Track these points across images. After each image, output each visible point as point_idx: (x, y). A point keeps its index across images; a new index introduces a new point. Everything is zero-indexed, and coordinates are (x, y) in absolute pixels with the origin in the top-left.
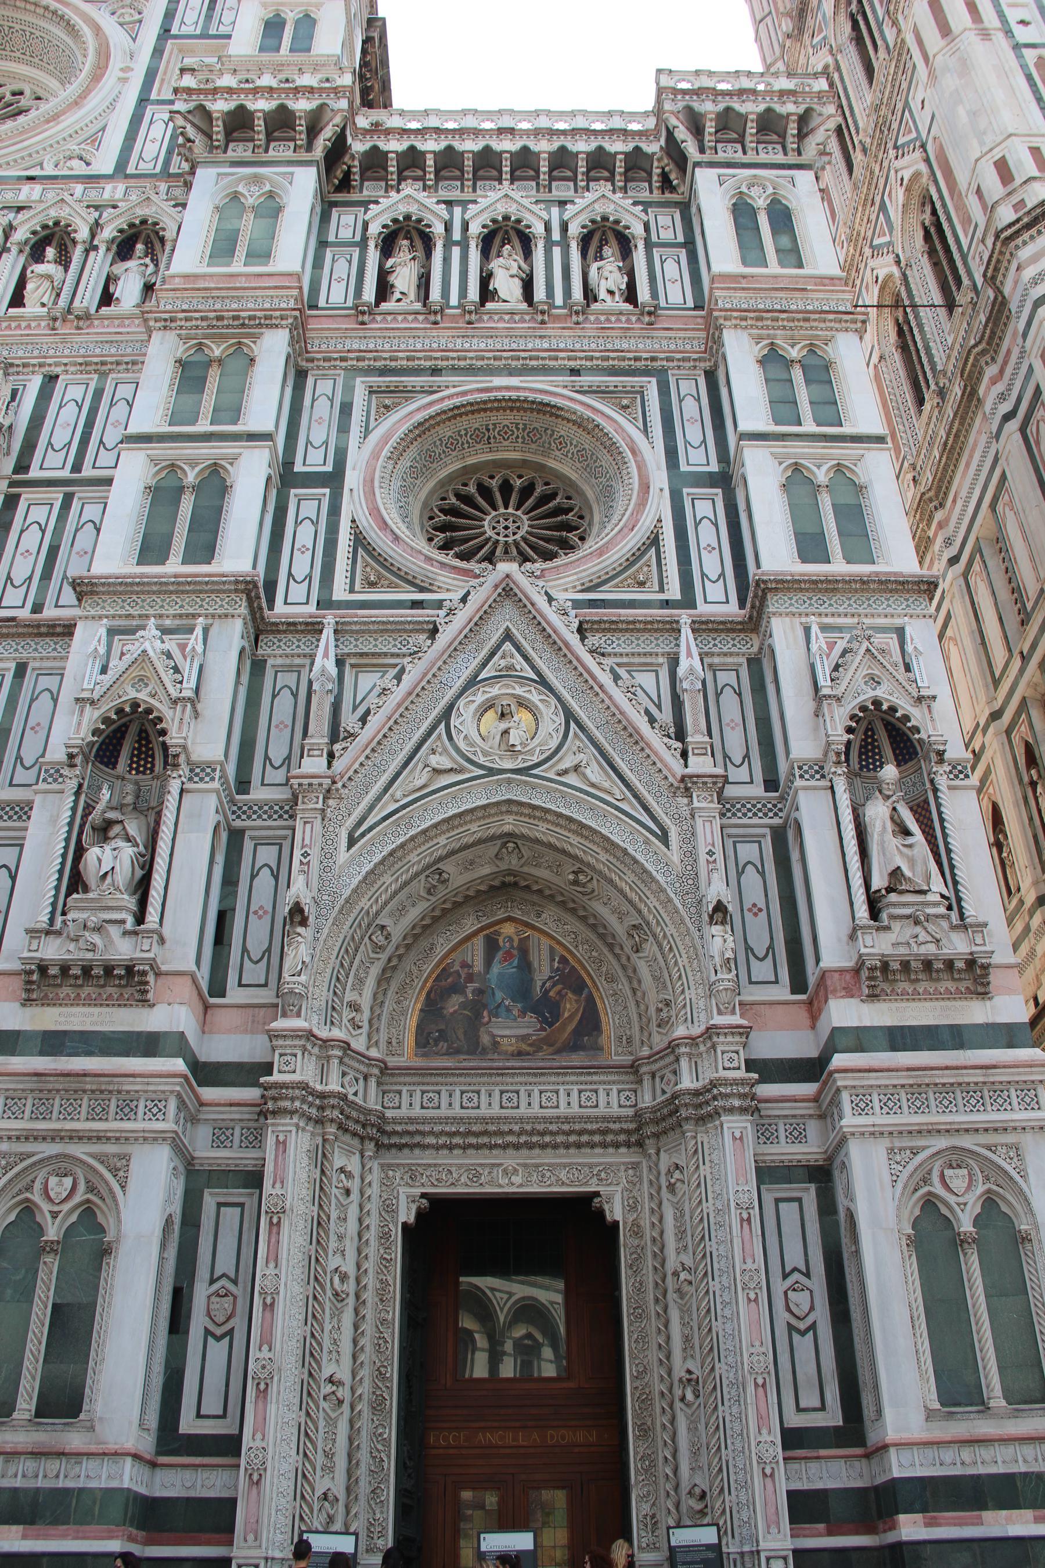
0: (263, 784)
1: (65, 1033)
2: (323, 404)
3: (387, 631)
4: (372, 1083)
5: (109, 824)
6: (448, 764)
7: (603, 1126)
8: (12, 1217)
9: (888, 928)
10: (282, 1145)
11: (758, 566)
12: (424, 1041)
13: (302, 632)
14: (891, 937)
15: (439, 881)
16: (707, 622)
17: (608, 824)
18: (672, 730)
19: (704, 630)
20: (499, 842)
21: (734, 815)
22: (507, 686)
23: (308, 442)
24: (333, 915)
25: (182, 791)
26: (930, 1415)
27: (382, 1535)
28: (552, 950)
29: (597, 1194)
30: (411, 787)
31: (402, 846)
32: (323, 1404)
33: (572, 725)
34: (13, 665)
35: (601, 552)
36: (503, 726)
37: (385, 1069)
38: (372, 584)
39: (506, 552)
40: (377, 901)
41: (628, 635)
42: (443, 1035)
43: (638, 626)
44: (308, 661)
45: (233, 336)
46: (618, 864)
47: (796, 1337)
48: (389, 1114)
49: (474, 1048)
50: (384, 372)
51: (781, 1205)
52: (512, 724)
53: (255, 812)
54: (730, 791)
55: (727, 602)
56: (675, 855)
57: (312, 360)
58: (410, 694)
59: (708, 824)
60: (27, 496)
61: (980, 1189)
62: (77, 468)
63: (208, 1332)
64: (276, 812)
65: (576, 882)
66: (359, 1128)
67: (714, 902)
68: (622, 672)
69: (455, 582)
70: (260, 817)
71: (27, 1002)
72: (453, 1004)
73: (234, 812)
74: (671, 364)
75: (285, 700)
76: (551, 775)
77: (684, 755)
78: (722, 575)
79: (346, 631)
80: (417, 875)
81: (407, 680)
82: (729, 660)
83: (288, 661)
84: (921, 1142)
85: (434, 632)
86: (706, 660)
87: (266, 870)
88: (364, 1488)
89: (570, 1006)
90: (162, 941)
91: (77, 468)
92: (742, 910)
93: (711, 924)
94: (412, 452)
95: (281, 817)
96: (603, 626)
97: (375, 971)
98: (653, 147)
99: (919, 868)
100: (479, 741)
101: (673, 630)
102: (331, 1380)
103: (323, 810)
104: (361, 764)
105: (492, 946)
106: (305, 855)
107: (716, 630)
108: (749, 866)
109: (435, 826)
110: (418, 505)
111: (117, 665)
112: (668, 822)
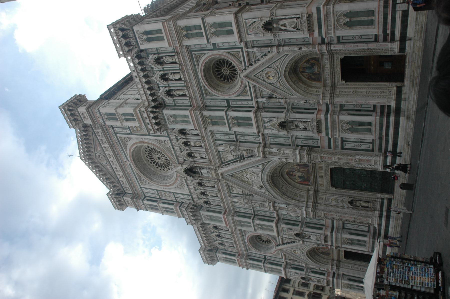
1: (325, 128)
2: (211, 103)
4: (326, 88)
5: (296, 126)
7: (331, 58)
8: (348, 131)
9: (303, 29)
10: (337, 102)
12: (318, 80)
14: (305, 29)
22: (264, 76)
23: (220, 104)
25: (290, 118)
26: (374, 28)
27: (385, 84)
28: (303, 64)
29: (340, 59)
32: (369, 94)
34: (269, 138)
37: (324, 86)
38: (246, 93)
42: (318, 78)
45: (205, 119)
47: (362, 38)
48: (330, 85)
49: (319, 74)
50: (203, 94)
51: (343, 39)
57: (203, 105)
58: (268, 89)
60: (239, 140)
61: (343, 17)
62: (233, 134)
63: (361, 107)
66: (333, 90)
71: (322, 132)
72: (313, 77)
74: (189, 50)
76: (279, 69)
80: (296, 86)
81: (265, 89)
83: (263, 104)
84: (336, 26)
88: (379, 87)
89: (312, 61)
90: (312, 119)
91: (233, 134)
94: (217, 88)
97: (310, 89)
98: (135, 55)
99: (292, 24)
102: (366, 93)
105: (304, 72)
106: (296, 101)
110: (225, 85)
111: (272, 128)
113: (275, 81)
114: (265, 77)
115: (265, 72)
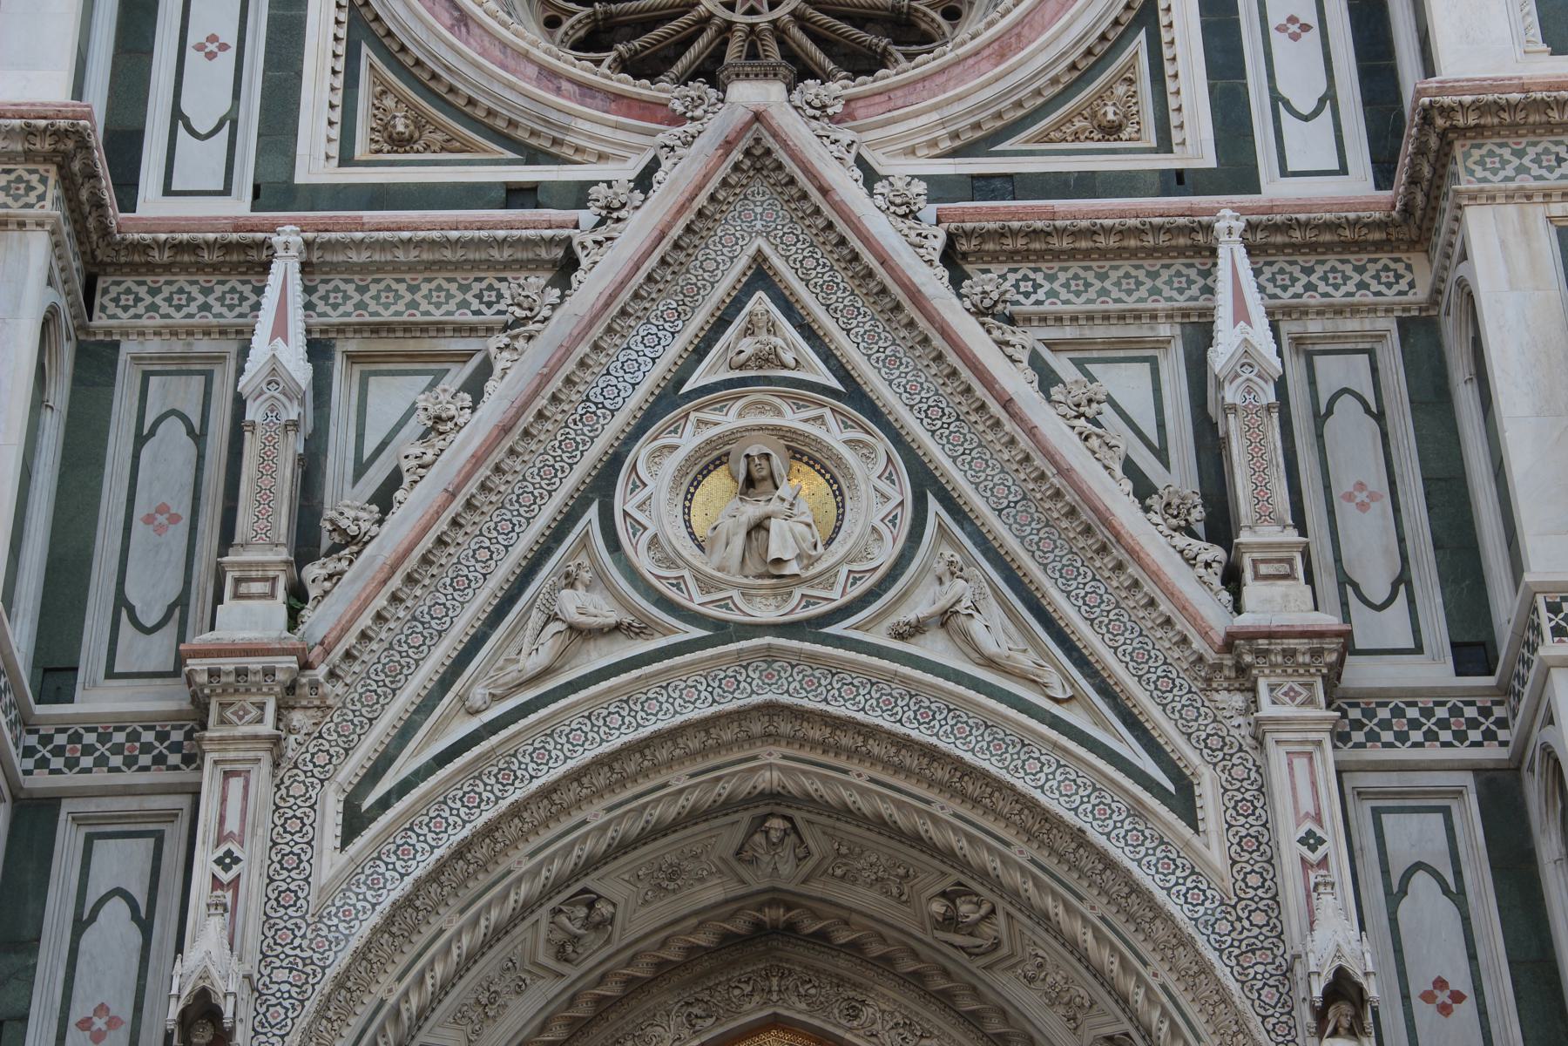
0: (110, 674)
3: (442, 265)
6: (607, 612)
11: (1429, 68)
13: (215, 268)
15: (587, 923)
16: (1286, 227)
17: (1032, 766)
18: (1197, 514)
19: (1280, 249)
20: (745, 817)
21: (1372, 737)
22: (760, 406)
24: (303, 1023)
30: (511, 674)
31: (490, 830)
33: (933, 505)
35: (1003, 47)
36: (751, 510)
38: (400, 143)
39: (753, 54)
40: (421, 980)
41: (1075, 267)
43: (1102, 242)
44: (231, 347)
46: (1061, 871)
52: (775, 506)
53: (88, 750)
54: (1361, 674)
55: (1343, 170)
56: (1214, 849)
58: (505, 430)
59: (1300, 764)
64: (146, 748)
65: (950, 922)
67: (1327, 975)
68: (1061, 364)
69: (621, 136)
70: (101, 761)
73: (28, 752)
75: (172, 445)
76: (879, 637)
77: (1232, 579)
78: (1329, 98)
79: (335, 267)
80: (528, 907)
81: (499, 395)
82: (1351, 324)
83: (178, 346)
85: (565, 267)
86: (1288, 327)
87: (118, 907)
92: (1406, 997)
93: (1320, 1033)
95: (160, 760)
96: (1009, 244)
100: (688, 550)
101: (1197, 250)
103: (276, 741)
104: (380, 617)
106: (227, 861)
107: (1313, 247)
108: (1420, 878)
109: (577, 776)
112: (1193, 757)
113: (670, 561)
114: (730, 419)
115: (833, 435)
